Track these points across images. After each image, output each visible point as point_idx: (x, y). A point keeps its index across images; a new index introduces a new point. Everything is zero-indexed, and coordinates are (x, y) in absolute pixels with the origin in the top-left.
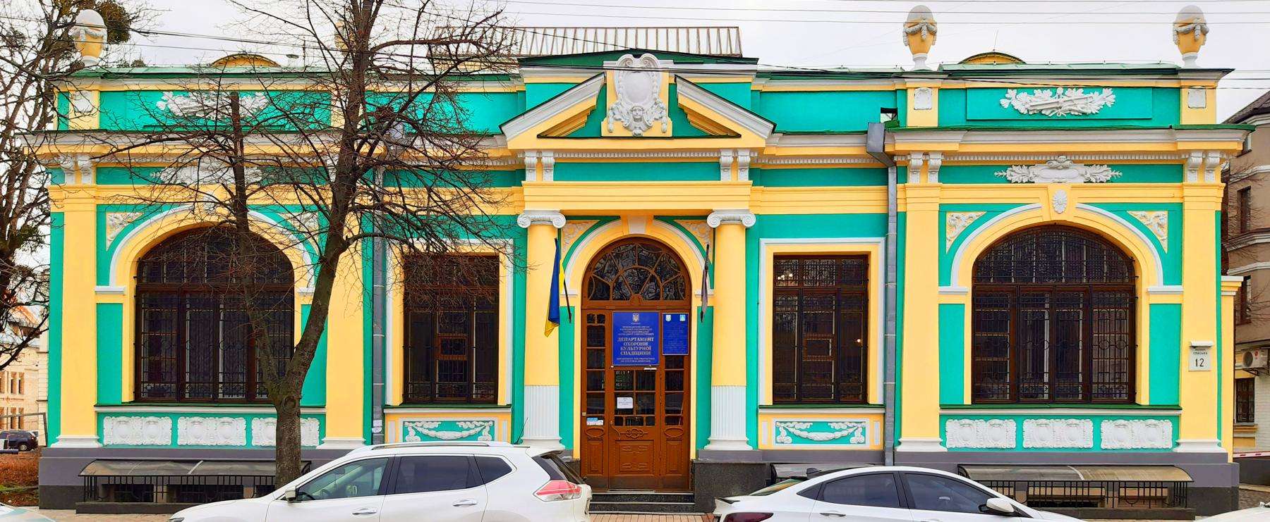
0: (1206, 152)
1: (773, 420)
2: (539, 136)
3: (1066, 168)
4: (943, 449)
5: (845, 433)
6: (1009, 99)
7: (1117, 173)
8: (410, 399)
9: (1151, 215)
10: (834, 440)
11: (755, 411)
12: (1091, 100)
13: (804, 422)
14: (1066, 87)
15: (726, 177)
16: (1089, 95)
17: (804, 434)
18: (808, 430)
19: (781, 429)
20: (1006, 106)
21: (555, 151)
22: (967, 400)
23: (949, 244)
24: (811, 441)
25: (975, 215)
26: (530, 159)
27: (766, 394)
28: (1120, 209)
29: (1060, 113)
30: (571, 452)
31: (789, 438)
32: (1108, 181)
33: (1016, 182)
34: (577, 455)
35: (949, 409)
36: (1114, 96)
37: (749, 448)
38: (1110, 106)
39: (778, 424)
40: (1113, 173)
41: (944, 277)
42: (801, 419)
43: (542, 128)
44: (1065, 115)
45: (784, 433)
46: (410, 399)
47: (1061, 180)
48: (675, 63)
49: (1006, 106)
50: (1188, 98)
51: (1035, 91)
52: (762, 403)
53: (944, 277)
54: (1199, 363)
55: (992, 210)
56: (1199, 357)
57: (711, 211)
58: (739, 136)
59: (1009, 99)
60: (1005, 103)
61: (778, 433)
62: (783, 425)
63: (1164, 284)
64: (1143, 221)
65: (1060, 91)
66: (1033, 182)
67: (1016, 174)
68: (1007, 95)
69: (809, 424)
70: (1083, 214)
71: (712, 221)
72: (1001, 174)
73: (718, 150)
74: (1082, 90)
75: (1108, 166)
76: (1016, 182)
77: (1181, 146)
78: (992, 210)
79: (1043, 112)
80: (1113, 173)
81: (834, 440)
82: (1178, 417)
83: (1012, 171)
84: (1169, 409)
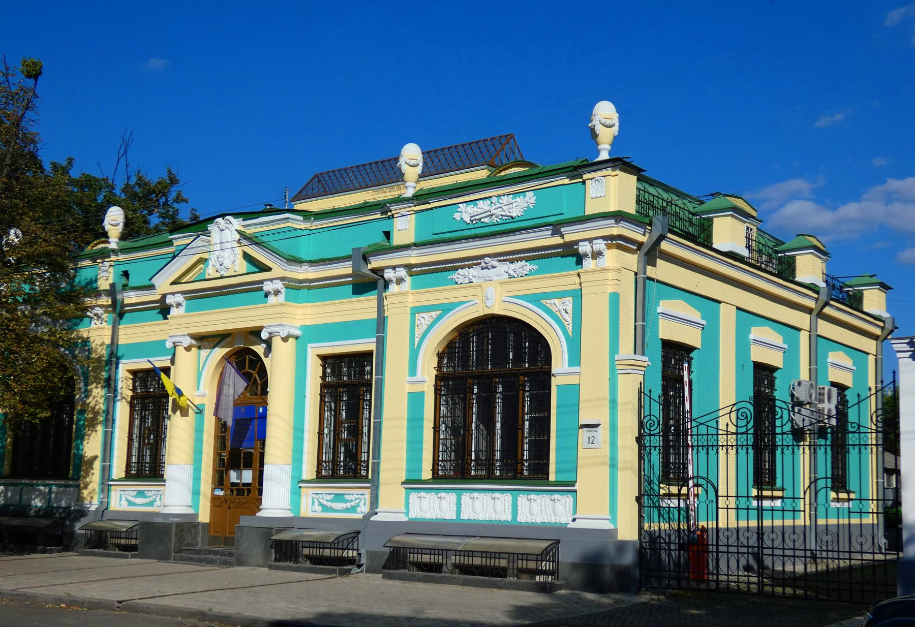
0: (590, 240)
1: (310, 491)
2: (173, 283)
3: (494, 267)
4: (403, 518)
5: (353, 504)
6: (461, 212)
7: (534, 267)
8: (129, 476)
9: (556, 301)
10: (347, 510)
11: (299, 483)
12: (515, 204)
13: (329, 494)
14: (499, 196)
15: (272, 299)
16: (515, 200)
17: (329, 504)
18: (332, 501)
19: (315, 500)
20: (458, 219)
21: (183, 293)
22: (427, 474)
23: (417, 340)
24: (332, 510)
25: (434, 314)
26: (170, 300)
27: (309, 470)
28: (536, 299)
29: (495, 220)
30: (196, 516)
31: (320, 507)
32: (526, 275)
33: (461, 283)
34: (204, 517)
35: (412, 483)
36: (535, 198)
37: (292, 515)
38: (532, 207)
39: (314, 495)
40: (531, 267)
41: (413, 371)
42: (327, 492)
43: (173, 279)
44: (499, 220)
45: (317, 503)
46: (129, 476)
47: (490, 279)
48: (244, 220)
49: (458, 219)
50: (592, 188)
51: (478, 202)
52: (304, 477)
53: (413, 371)
54: (591, 440)
55: (446, 309)
56: (591, 434)
57: (262, 327)
58: (269, 269)
59: (461, 212)
60: (457, 216)
61: (313, 503)
62: (317, 496)
63: (569, 366)
64: (554, 309)
65: (494, 199)
66: (472, 282)
67: (461, 275)
68: (458, 210)
69: (332, 496)
70: (512, 306)
71: (264, 335)
72: (452, 277)
73: (261, 282)
74: (511, 196)
75: (526, 261)
76: (461, 283)
77: (569, 238)
78: (446, 309)
79: (482, 220)
80: (531, 267)
81: (347, 510)
82: (575, 491)
83: (458, 274)
84: (567, 486)
